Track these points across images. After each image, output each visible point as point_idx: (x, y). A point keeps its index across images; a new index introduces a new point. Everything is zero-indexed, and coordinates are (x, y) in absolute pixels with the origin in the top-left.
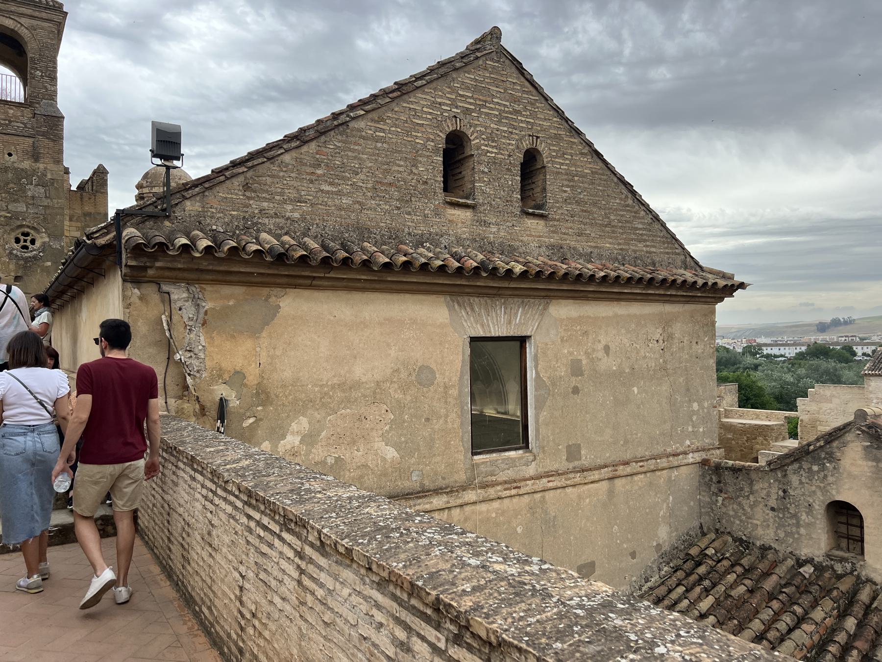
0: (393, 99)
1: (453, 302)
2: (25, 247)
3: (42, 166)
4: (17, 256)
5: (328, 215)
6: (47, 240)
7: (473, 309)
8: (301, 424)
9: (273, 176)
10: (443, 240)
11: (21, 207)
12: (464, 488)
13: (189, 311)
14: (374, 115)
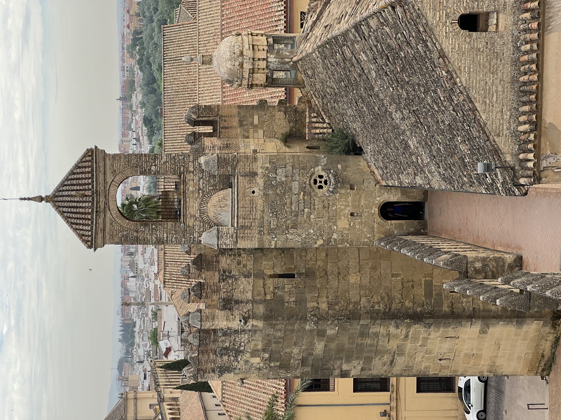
0: (449, 62)
1: (547, 30)
2: (326, 182)
3: (260, 171)
4: (334, 188)
5: (507, 98)
6: (320, 167)
7: (551, 17)
9: (492, 123)
10: (515, 34)
11: (295, 186)
13: (551, 160)
14: (458, 72)
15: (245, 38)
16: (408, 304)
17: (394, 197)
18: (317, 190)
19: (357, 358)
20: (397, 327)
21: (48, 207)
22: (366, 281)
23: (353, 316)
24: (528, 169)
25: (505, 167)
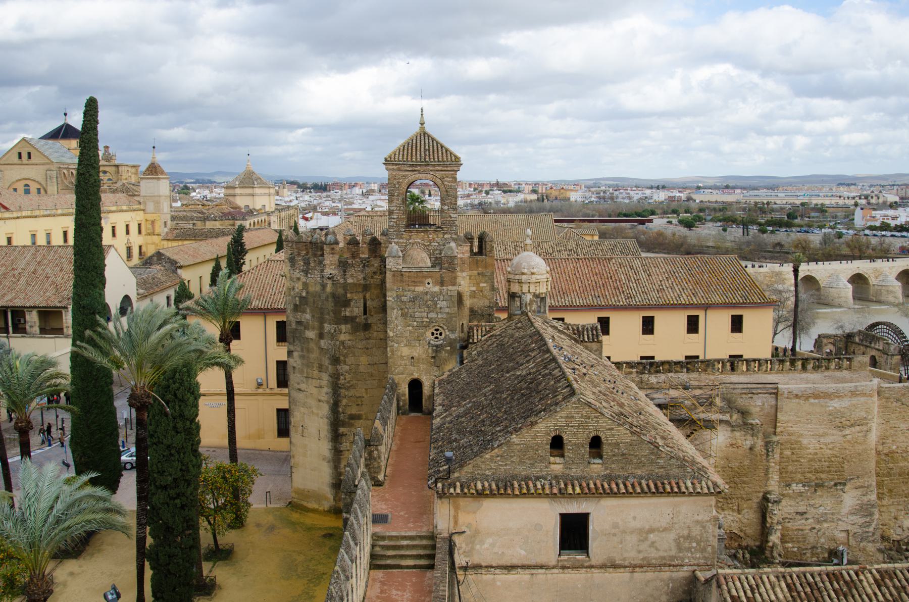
8: (490, 540)
12: (553, 568)
15: (545, 276)
16: (344, 402)
17: (426, 390)
18: (430, 331)
19: (303, 364)
20: (327, 393)
21: (416, 129)
22: (362, 369)
23: (336, 361)
24: (449, 490)
25: (449, 472)
